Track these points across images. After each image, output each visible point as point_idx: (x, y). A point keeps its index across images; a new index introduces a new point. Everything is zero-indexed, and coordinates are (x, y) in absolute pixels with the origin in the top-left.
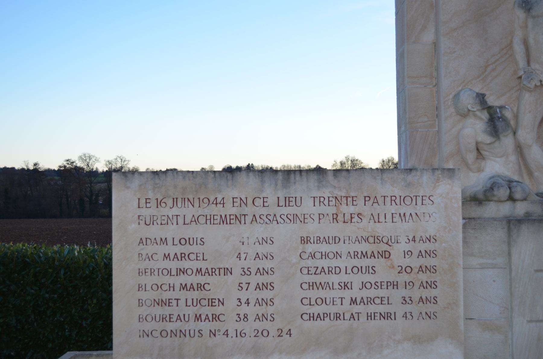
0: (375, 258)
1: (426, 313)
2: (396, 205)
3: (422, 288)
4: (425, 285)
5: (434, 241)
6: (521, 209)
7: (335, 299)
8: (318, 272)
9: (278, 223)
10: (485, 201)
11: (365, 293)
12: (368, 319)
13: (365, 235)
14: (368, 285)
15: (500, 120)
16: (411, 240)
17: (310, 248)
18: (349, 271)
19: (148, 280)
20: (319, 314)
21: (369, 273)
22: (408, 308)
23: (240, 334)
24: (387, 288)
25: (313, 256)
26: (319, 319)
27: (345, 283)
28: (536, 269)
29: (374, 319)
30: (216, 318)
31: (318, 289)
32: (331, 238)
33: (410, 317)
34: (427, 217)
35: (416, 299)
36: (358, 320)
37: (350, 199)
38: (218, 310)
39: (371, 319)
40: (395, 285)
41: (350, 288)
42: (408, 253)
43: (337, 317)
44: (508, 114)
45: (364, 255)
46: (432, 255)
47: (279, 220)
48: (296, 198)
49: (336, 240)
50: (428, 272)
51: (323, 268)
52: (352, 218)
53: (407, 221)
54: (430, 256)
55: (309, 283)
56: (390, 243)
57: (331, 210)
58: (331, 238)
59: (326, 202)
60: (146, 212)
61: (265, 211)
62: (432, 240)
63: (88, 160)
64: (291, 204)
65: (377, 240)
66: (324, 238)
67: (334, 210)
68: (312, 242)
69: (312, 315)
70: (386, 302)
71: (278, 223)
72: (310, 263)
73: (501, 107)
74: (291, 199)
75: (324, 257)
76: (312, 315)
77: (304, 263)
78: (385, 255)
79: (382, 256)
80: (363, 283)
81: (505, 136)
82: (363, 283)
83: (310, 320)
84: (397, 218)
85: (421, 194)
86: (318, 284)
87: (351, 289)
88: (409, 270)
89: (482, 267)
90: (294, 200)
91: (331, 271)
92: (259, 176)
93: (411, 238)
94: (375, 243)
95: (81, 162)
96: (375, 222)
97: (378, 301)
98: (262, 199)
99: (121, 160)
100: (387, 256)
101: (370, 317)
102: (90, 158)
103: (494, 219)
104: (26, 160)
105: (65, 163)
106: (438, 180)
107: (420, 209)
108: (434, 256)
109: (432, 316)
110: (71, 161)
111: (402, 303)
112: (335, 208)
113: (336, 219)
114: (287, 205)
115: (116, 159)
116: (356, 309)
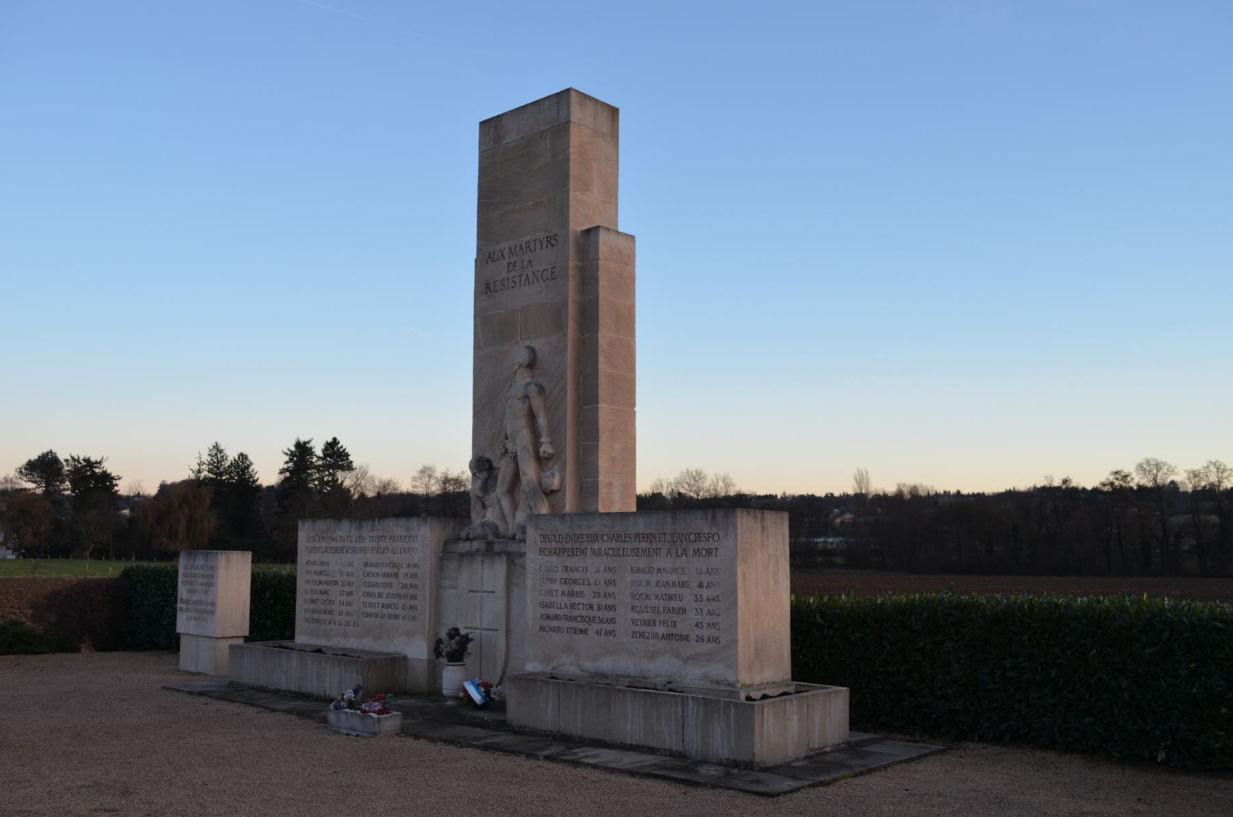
17: (368, 569)
19: (309, 587)
22: (405, 612)
23: (340, 624)
30: (331, 612)
38: (333, 607)
40: (399, 596)
60: (310, 545)
61: (350, 545)
63: (1155, 471)
65: (393, 565)
72: (367, 579)
78: (396, 575)
95: (1140, 476)
99: (1218, 469)
101: (389, 616)
102: (1158, 467)
104: (1048, 475)
105: (1112, 478)
110: (1123, 474)
115: (1208, 467)
116: (385, 611)
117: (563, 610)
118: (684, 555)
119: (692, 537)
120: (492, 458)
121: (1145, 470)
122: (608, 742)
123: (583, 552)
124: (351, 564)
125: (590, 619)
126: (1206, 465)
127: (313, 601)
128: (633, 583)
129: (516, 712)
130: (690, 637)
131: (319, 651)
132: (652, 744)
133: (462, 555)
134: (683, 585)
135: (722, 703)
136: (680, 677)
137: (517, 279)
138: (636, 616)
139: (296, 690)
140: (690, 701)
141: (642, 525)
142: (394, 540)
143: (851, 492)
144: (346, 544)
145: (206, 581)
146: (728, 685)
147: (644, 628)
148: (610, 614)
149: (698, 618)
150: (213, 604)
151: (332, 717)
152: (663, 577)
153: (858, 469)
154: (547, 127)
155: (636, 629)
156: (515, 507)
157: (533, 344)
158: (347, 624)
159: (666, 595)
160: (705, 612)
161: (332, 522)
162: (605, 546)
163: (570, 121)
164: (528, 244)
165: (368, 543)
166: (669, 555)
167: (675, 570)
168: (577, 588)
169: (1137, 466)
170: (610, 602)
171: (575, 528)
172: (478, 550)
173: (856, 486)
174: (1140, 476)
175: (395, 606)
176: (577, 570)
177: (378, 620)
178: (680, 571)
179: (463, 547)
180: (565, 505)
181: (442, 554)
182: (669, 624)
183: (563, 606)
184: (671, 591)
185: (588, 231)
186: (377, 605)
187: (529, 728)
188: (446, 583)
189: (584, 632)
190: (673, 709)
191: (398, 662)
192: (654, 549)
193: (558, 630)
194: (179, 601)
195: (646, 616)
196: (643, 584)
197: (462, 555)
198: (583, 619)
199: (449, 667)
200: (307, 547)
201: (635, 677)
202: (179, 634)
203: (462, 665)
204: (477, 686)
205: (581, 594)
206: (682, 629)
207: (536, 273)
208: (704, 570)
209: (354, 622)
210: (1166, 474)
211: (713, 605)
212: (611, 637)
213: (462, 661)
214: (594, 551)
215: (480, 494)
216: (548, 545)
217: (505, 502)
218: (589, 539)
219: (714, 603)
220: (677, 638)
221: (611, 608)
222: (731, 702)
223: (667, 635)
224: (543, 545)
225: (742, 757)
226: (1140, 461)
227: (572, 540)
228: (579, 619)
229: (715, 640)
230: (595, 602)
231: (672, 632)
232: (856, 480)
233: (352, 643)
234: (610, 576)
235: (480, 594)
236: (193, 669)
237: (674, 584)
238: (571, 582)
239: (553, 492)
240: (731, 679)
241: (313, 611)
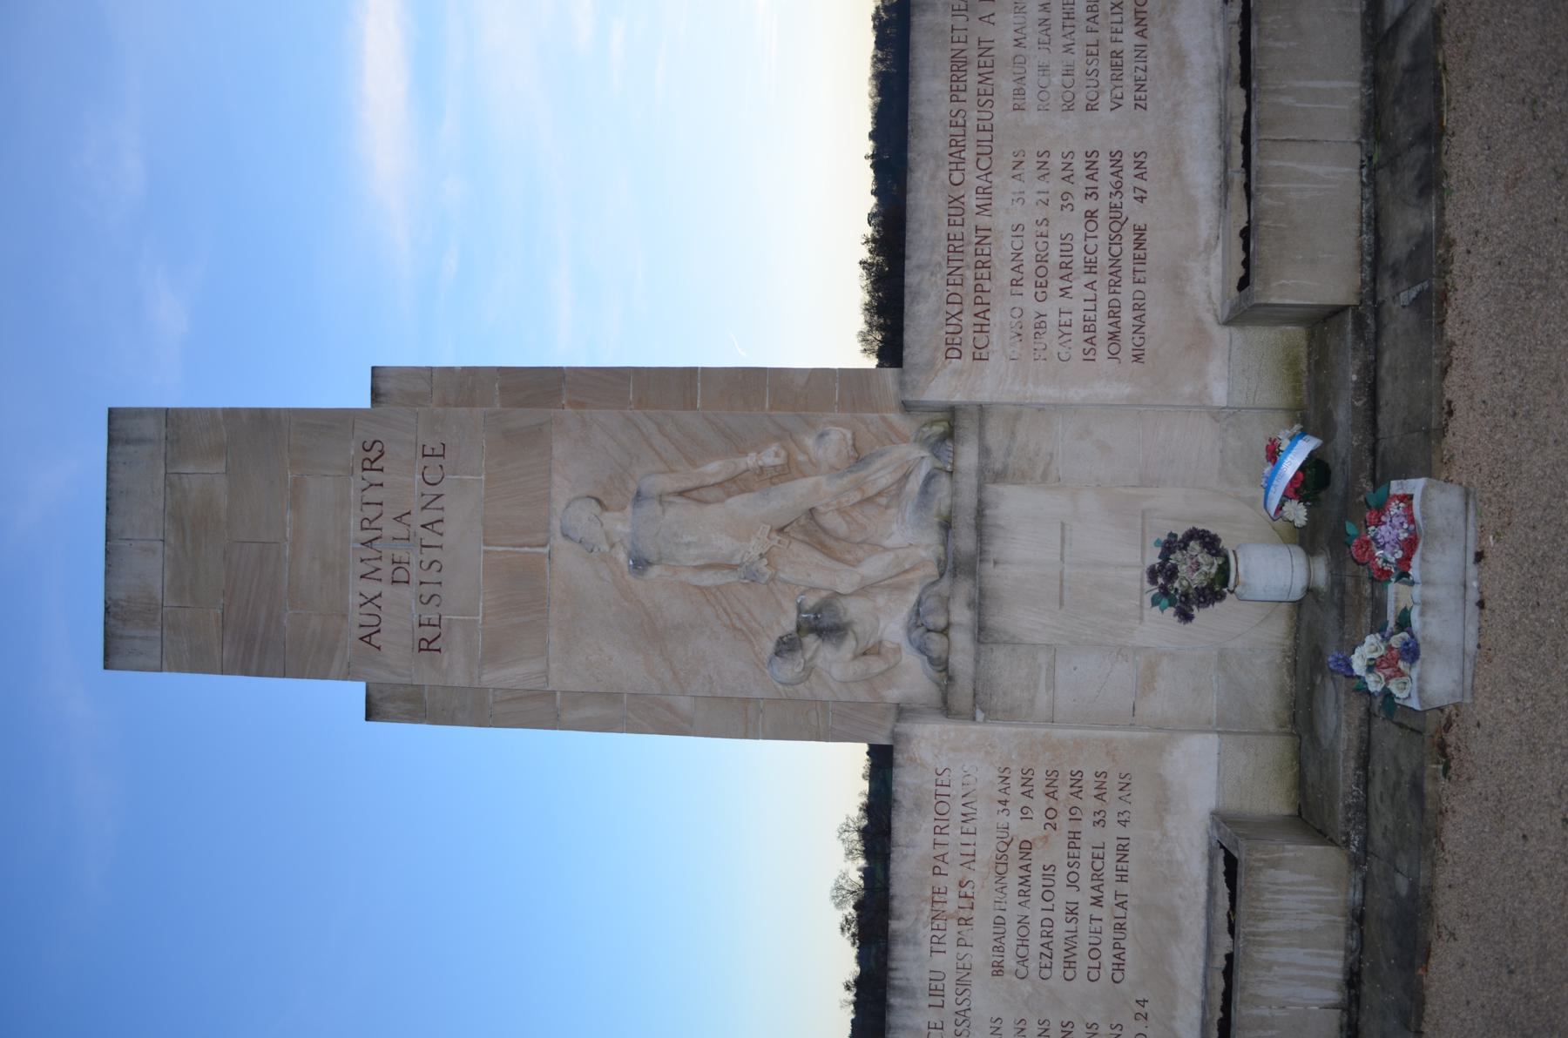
0: (1029, 865)
1: (1121, 790)
2: (948, 826)
3: (1080, 795)
4: (1077, 790)
5: (1007, 771)
6: (961, 615)
7: (1093, 930)
8: (1048, 952)
9: (969, 1009)
10: (948, 673)
11: (1085, 882)
12: (1126, 881)
13: (993, 877)
14: (1073, 877)
15: (819, 616)
16: (1004, 807)
17: (1010, 963)
18: (1049, 905)
20: (1115, 956)
21: (1053, 875)
22: (1111, 818)
24: (1079, 848)
25: (1023, 959)
26: (1122, 956)
27: (1067, 913)
28: (1058, 607)
29: (1126, 871)
31: (1074, 954)
32: (996, 930)
33: (1126, 814)
34: (970, 779)
35: (1097, 805)
36: (1126, 895)
37: (937, 898)
39: (1127, 876)
40: (1074, 836)
41: (1076, 906)
42: (1025, 812)
43: (1120, 927)
44: (811, 601)
45: (1025, 880)
46: (1029, 775)
47: (964, 1006)
48: (931, 980)
49: (1000, 922)
50: (1055, 784)
51: (1042, 945)
52: (966, 896)
53: (974, 811)
54: (1030, 779)
55: (1065, 968)
56: (1008, 840)
57: (952, 927)
58: (996, 930)
59: (939, 934)
62: (1006, 774)
63: (844, 892)
64: (940, 987)
65: (1001, 859)
66: (995, 940)
67: (953, 923)
68: (1001, 959)
69: (1116, 967)
70: (1100, 851)
71: (969, 1009)
72: (1033, 965)
73: (800, 609)
74: (933, 987)
75: (1025, 943)
76: (1116, 967)
77: (1034, 974)
78: (1026, 847)
79: (1028, 853)
80: (1068, 886)
81: (845, 613)
82: (1068, 886)
83: (1123, 970)
84: (970, 827)
85: (934, 787)
86: (1067, 954)
87: (1077, 903)
88: (1051, 814)
89: (1052, 685)
90: (934, 983)
91: (1048, 933)
92: (893, 1033)
93: (1001, 807)
94: (1007, 864)
95: (847, 906)
96: (974, 861)
97: (1098, 864)
98: (931, 1030)
100: (1028, 846)
101: (1122, 877)
102: (840, 888)
103: (977, 661)
104: (839, 1004)
105: (847, 935)
106: (912, 760)
107: (957, 790)
108: (1031, 772)
109: (1126, 780)
111: (1103, 826)
112: (949, 921)
113: (966, 920)
114: (941, 993)
115: (843, 840)
116: (1109, 898)
117: (1098, 293)
122: (1364, 8)
123: (984, 235)
128: (1044, 108)
133: (982, 633)
138: (1105, 100)
147: (1128, 81)
148: (1104, 163)
154: (162, 472)
155: (1129, 100)
162: (973, 179)
164: (366, 524)
166: (993, 19)
168: (1055, 256)
170: (1079, 165)
171: (937, 258)
174: (847, 906)
177: (1132, 919)
182: (1117, 18)
183: (1090, 294)
189: (1140, 232)
192: (980, 55)
193: (1138, 307)
195: (1105, 73)
197: (982, 633)
199: (1240, 570)
205: (1066, 239)
214: (983, 208)
216: (968, 335)
217: (873, 567)
218: (959, 220)
221: (1091, 157)
223: (1137, 25)
224: (968, 350)
226: (833, 905)
227: (958, 268)
228: (1116, 249)
230: (1082, 205)
231: (1133, 12)
238: (1041, 272)
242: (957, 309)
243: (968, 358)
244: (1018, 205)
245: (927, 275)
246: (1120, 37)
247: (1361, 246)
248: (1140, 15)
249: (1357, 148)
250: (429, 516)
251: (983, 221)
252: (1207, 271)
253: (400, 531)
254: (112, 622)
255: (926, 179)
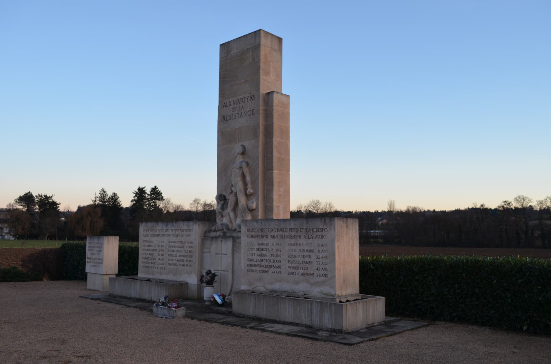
17: (171, 244)
19: (144, 252)
22: (187, 263)
23: (158, 268)
30: (154, 263)
38: (155, 261)
40: (184, 256)
60: (145, 233)
61: (162, 233)
63: (522, 201)
65: (182, 242)
72: (170, 249)
78: (183, 247)
95: (516, 203)
101: (180, 265)
104: (475, 202)
105: (503, 204)
110: (508, 202)
115: (546, 199)
116: (178, 263)
117: (257, 262)
118: (312, 238)
119: (315, 230)
120: (226, 195)
121: (518, 201)
123: (266, 236)
124: (163, 242)
125: (269, 266)
126: (545, 198)
127: (146, 258)
128: (289, 250)
129: (236, 307)
130: (314, 274)
131: (149, 280)
132: (297, 322)
134: (311, 251)
135: (328, 304)
136: (310, 292)
137: (237, 115)
138: (290, 265)
139: (139, 298)
140: (314, 302)
141: (292, 224)
142: (182, 231)
143: (386, 210)
144: (160, 233)
145: (99, 249)
146: (331, 296)
147: (293, 270)
148: (278, 264)
149: (317, 266)
150: (102, 260)
151: (155, 309)
152: (302, 248)
153: (390, 200)
154: (250, 47)
155: (290, 271)
156: (236, 216)
157: (244, 144)
158: (161, 268)
159: (303, 255)
160: (321, 263)
161: (155, 223)
162: (276, 234)
163: (260, 44)
164: (242, 99)
165: (170, 233)
166: (305, 238)
167: (307, 244)
168: (264, 253)
169: (514, 199)
170: (278, 258)
171: (263, 226)
172: (219, 236)
173: (389, 207)
174: (516, 203)
175: (183, 261)
176: (264, 244)
177: (175, 267)
178: (310, 245)
179: (213, 234)
180: (258, 216)
181: (203, 237)
182: (305, 269)
183: (257, 260)
184: (306, 254)
185: (269, 93)
186: (175, 260)
187: (242, 314)
188: (205, 250)
189: (267, 272)
190: (307, 306)
191: (184, 285)
192: (298, 235)
193: (255, 271)
194: (86, 258)
195: (295, 265)
196: (293, 250)
198: (267, 266)
200: (143, 234)
201: (289, 292)
202: (87, 273)
203: (212, 287)
204: (219, 296)
205: (265, 255)
206: (311, 271)
207: (245, 112)
208: (321, 245)
209: (165, 268)
210: (527, 202)
211: (325, 260)
212: (279, 274)
213: (212, 285)
214: (271, 236)
215: (220, 211)
216: (251, 234)
217: (232, 214)
218: (269, 231)
219: (325, 259)
220: (308, 275)
222: (332, 303)
224: (249, 234)
225: (337, 328)
226: (516, 197)
228: (265, 266)
229: (326, 276)
230: (272, 259)
231: (306, 272)
232: (389, 205)
233: (164, 277)
234: (278, 247)
235: (220, 255)
236: (93, 288)
237: (307, 251)
239: (253, 210)
240: (333, 293)
241: (146, 263)
242: (255, 231)
243: (247, 233)
244: (272, 244)
245: (260, 224)
246: (302, 269)
247: (240, 314)
248: (306, 274)
249: (255, 316)
250: (243, 113)
251: (269, 236)
252: (261, 286)
253: (241, 107)
254: (227, 44)
255: (276, 223)
